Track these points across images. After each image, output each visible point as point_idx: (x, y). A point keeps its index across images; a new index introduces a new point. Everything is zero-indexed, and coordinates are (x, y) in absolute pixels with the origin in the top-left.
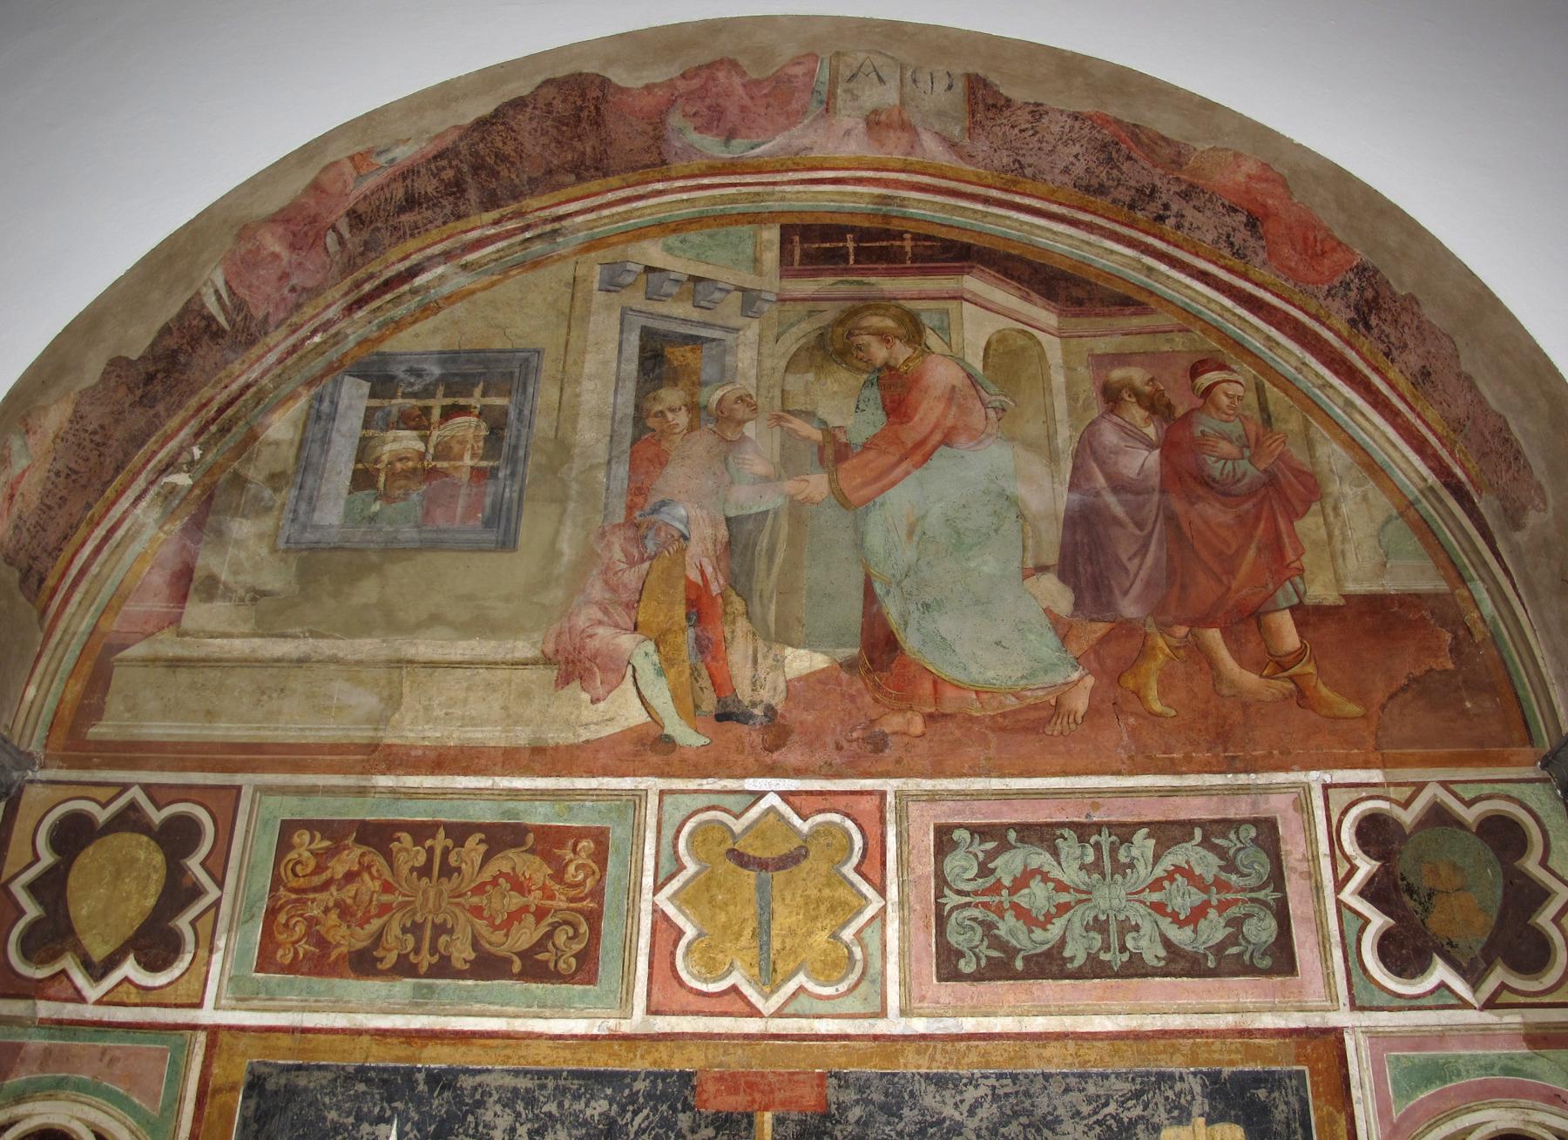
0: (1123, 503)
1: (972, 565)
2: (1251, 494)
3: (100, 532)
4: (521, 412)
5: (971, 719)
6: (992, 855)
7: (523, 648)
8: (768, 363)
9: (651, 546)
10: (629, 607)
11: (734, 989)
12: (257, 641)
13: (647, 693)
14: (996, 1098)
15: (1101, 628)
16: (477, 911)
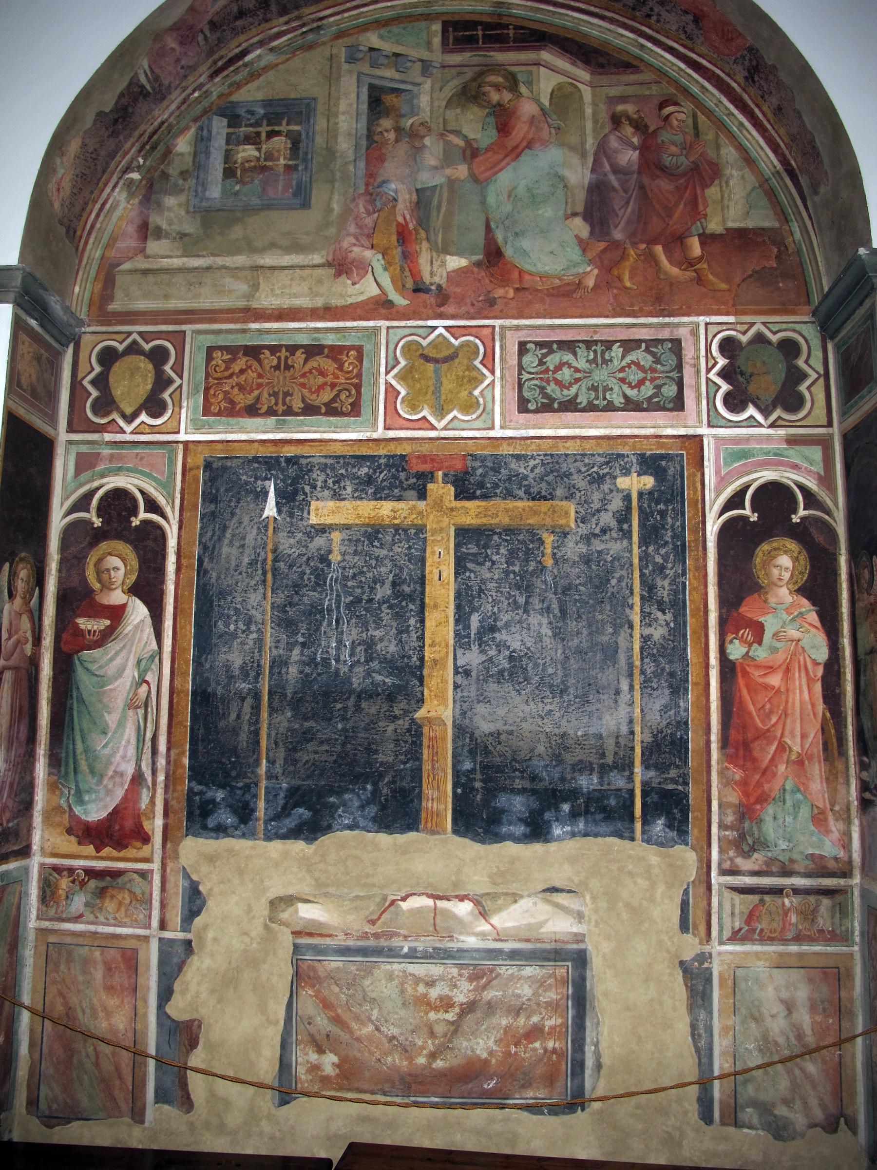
0: (618, 180)
1: (540, 212)
2: (684, 174)
3: (98, 206)
4: (308, 134)
5: (537, 290)
6: (545, 356)
8: (436, 104)
9: (378, 204)
10: (369, 236)
11: (424, 418)
12: (185, 259)
13: (379, 280)
14: (543, 464)
15: (602, 245)
16: (303, 385)
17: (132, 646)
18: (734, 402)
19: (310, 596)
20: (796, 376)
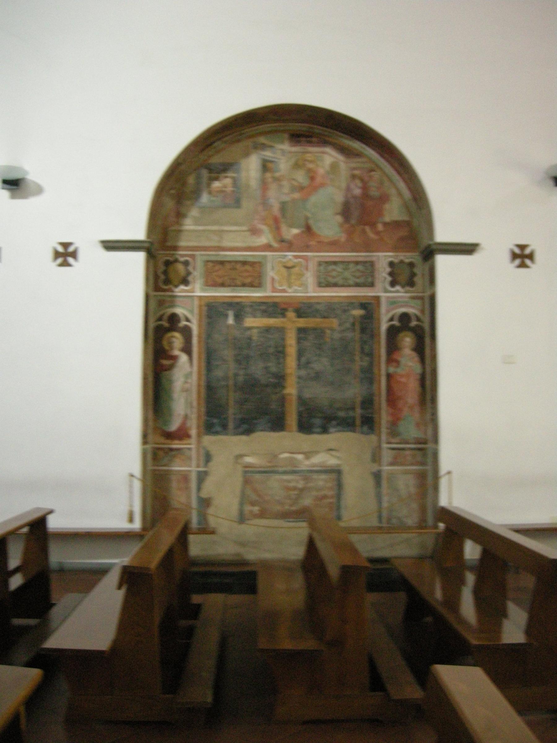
7: (244, 228)
18: (393, 284)
19: (245, 352)
20: (413, 275)
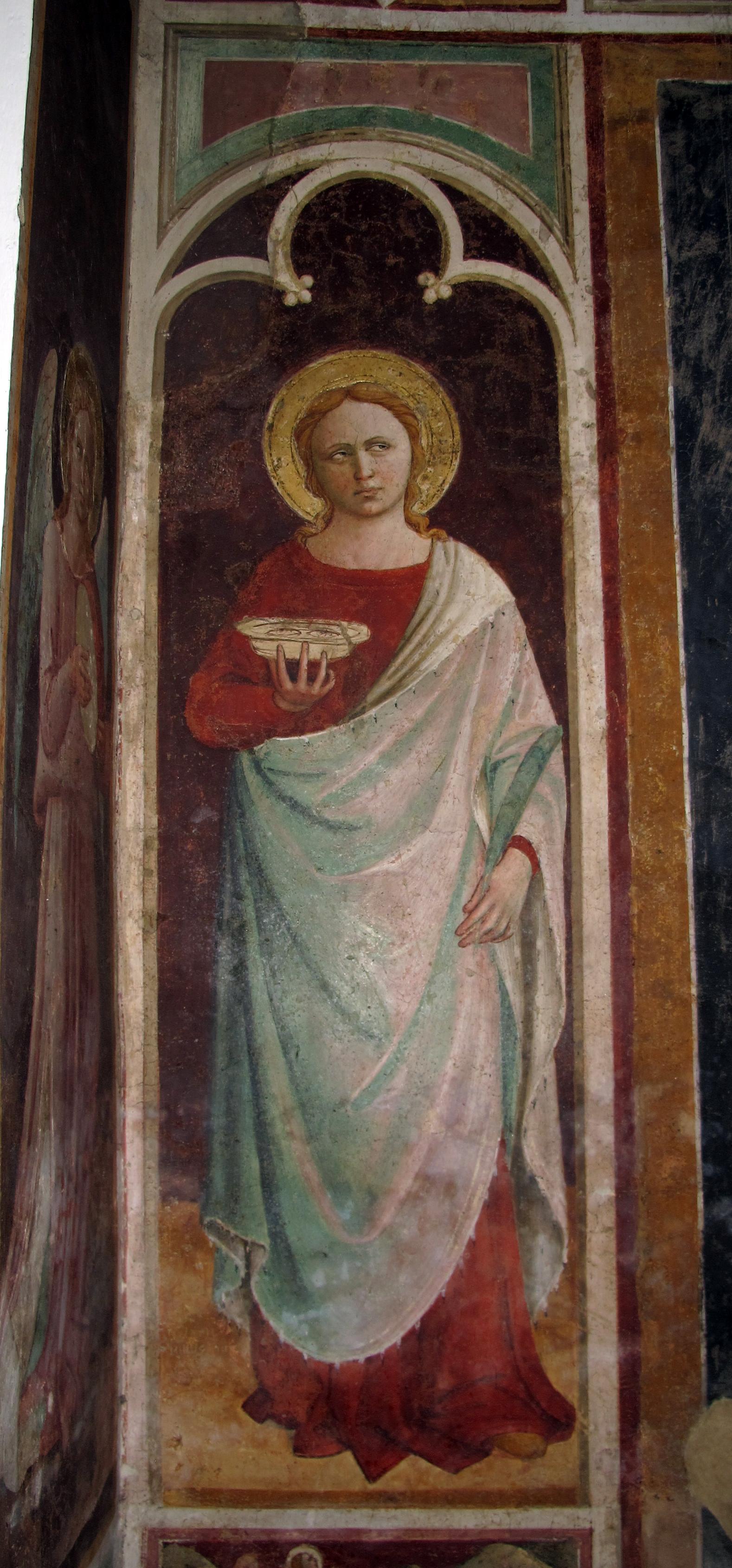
17: (458, 714)
